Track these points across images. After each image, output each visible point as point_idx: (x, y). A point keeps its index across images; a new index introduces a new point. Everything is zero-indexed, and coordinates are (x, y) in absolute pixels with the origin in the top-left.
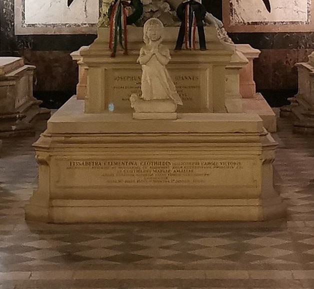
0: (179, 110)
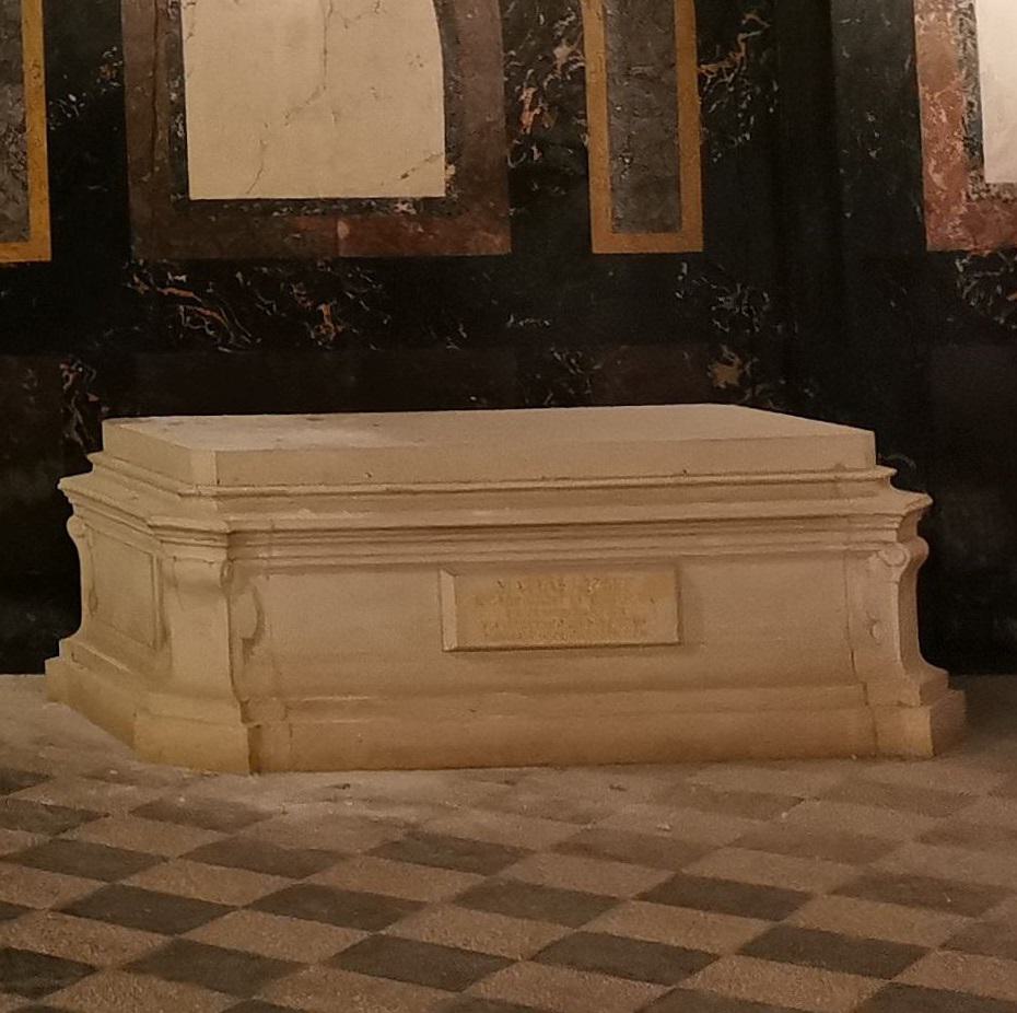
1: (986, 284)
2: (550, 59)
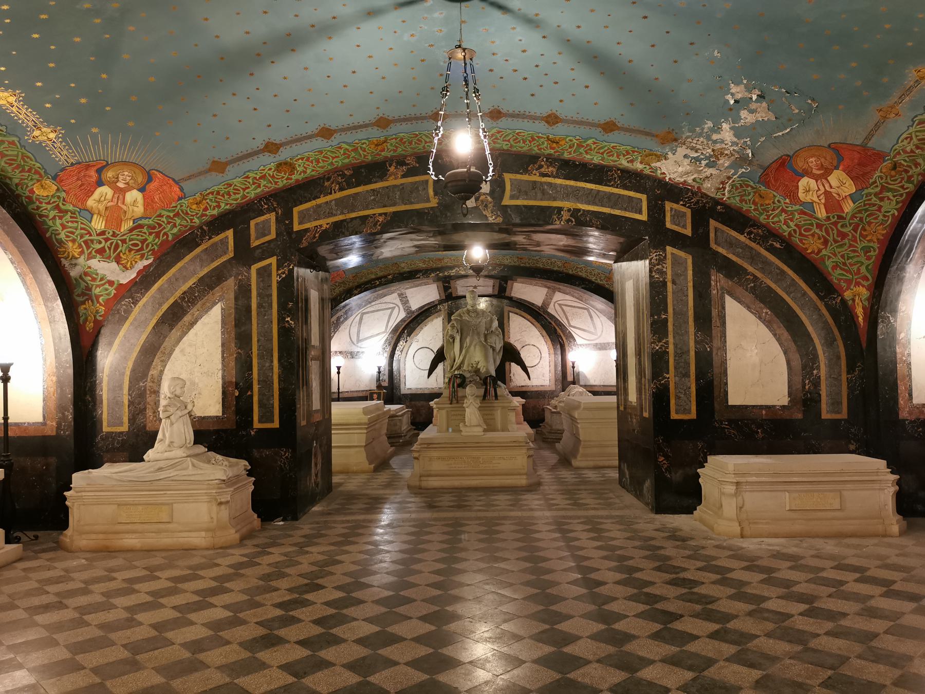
0: (485, 431)
1: (913, 427)
2: (812, 373)
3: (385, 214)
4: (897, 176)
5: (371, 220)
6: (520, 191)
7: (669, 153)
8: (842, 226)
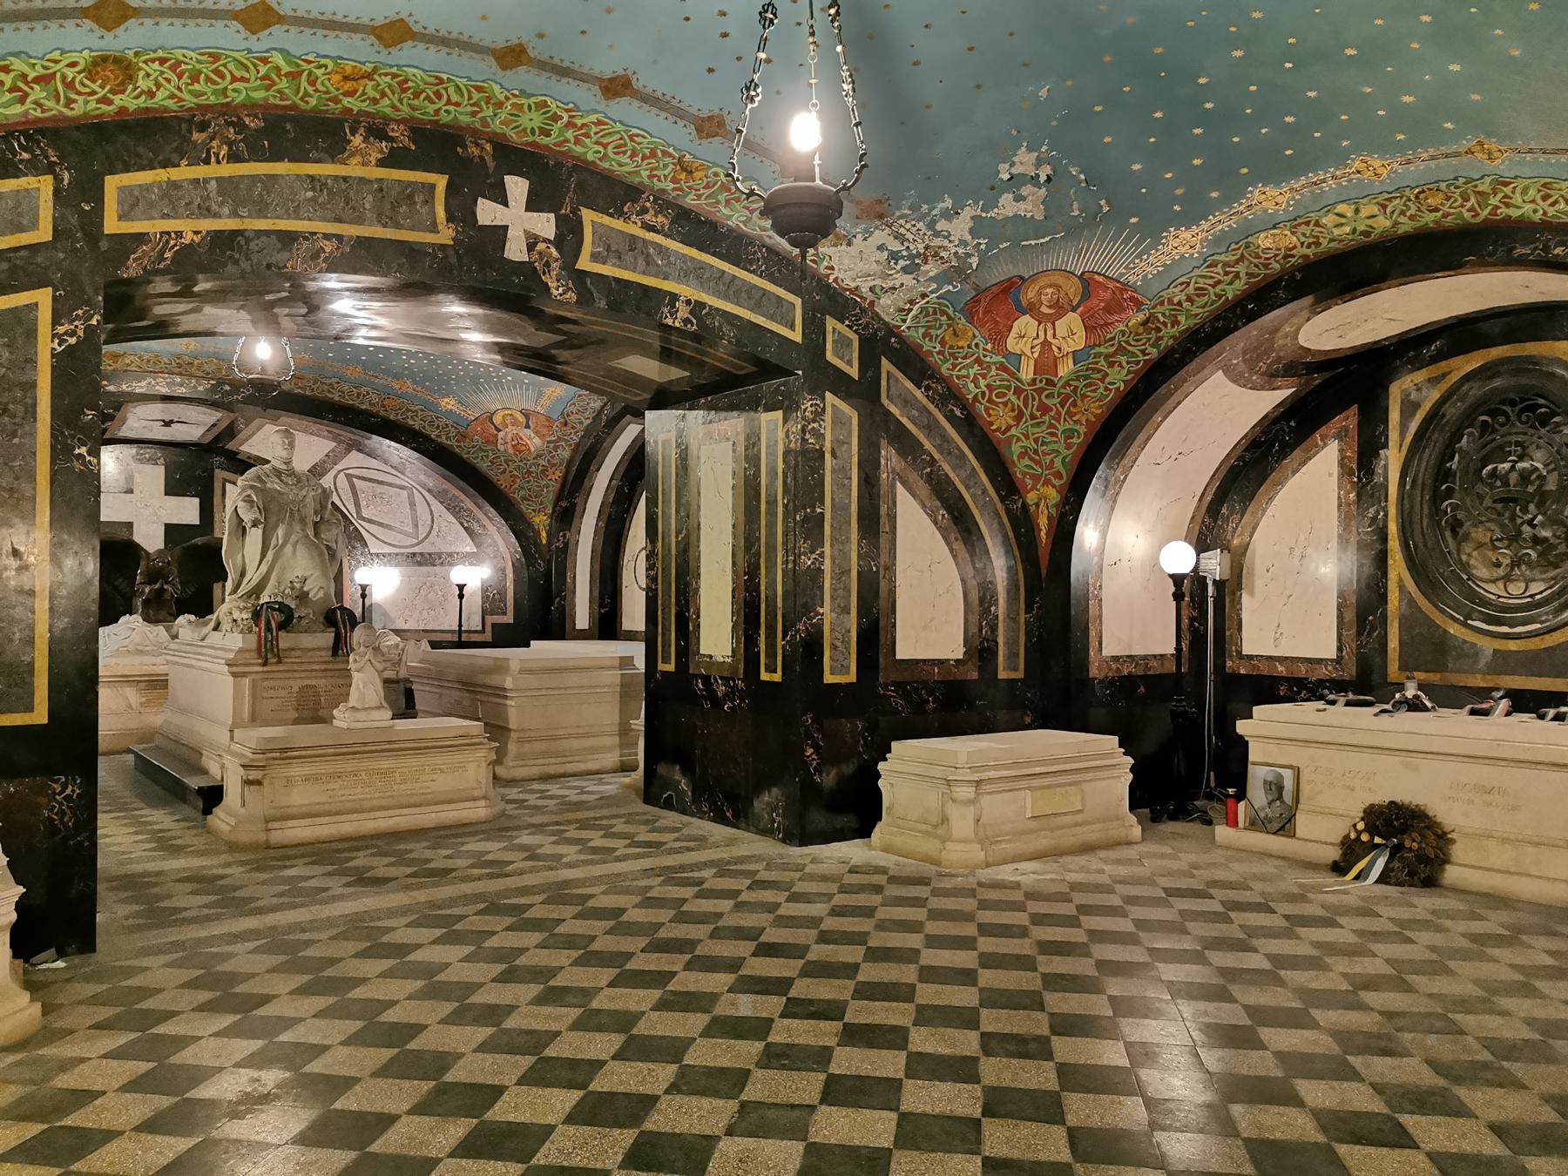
3: (339, 238)
4: (1144, 336)
5: (306, 244)
6: (608, 249)
7: (859, 236)
8: (1047, 397)
